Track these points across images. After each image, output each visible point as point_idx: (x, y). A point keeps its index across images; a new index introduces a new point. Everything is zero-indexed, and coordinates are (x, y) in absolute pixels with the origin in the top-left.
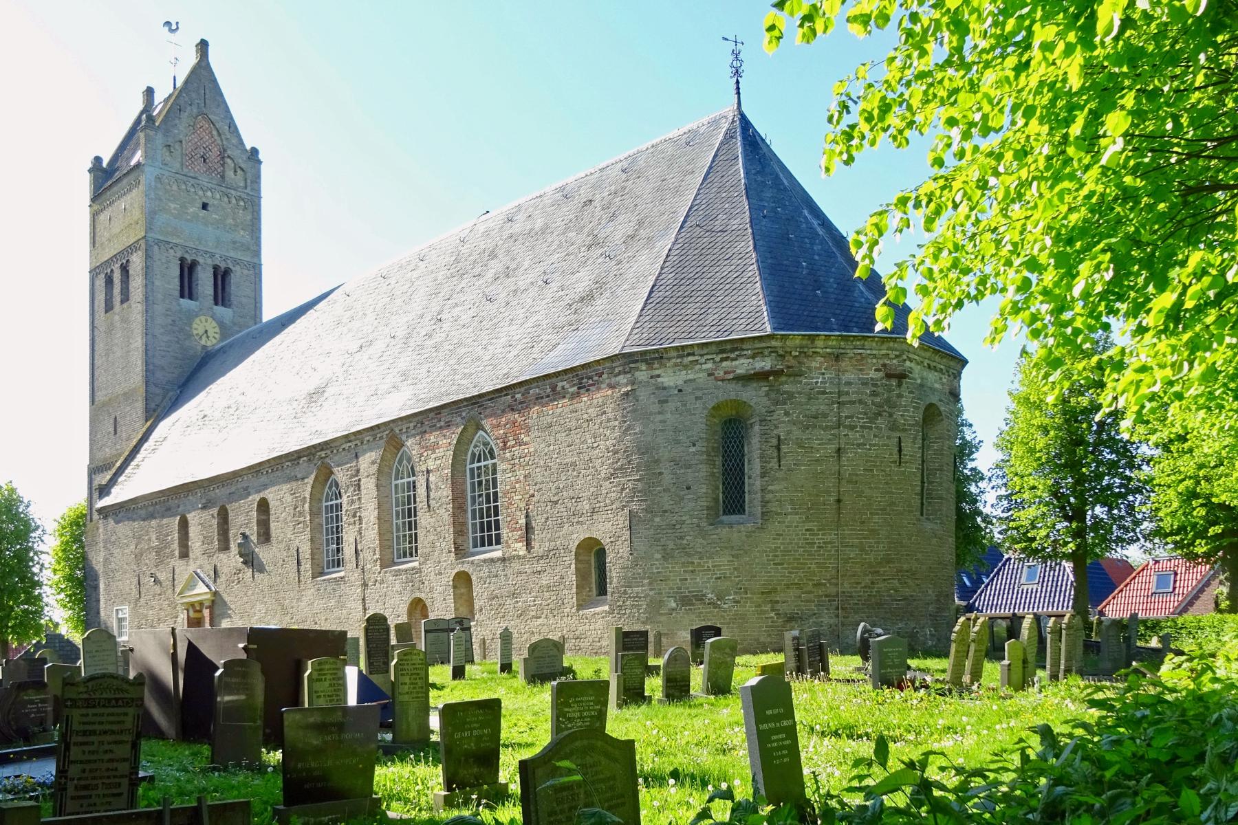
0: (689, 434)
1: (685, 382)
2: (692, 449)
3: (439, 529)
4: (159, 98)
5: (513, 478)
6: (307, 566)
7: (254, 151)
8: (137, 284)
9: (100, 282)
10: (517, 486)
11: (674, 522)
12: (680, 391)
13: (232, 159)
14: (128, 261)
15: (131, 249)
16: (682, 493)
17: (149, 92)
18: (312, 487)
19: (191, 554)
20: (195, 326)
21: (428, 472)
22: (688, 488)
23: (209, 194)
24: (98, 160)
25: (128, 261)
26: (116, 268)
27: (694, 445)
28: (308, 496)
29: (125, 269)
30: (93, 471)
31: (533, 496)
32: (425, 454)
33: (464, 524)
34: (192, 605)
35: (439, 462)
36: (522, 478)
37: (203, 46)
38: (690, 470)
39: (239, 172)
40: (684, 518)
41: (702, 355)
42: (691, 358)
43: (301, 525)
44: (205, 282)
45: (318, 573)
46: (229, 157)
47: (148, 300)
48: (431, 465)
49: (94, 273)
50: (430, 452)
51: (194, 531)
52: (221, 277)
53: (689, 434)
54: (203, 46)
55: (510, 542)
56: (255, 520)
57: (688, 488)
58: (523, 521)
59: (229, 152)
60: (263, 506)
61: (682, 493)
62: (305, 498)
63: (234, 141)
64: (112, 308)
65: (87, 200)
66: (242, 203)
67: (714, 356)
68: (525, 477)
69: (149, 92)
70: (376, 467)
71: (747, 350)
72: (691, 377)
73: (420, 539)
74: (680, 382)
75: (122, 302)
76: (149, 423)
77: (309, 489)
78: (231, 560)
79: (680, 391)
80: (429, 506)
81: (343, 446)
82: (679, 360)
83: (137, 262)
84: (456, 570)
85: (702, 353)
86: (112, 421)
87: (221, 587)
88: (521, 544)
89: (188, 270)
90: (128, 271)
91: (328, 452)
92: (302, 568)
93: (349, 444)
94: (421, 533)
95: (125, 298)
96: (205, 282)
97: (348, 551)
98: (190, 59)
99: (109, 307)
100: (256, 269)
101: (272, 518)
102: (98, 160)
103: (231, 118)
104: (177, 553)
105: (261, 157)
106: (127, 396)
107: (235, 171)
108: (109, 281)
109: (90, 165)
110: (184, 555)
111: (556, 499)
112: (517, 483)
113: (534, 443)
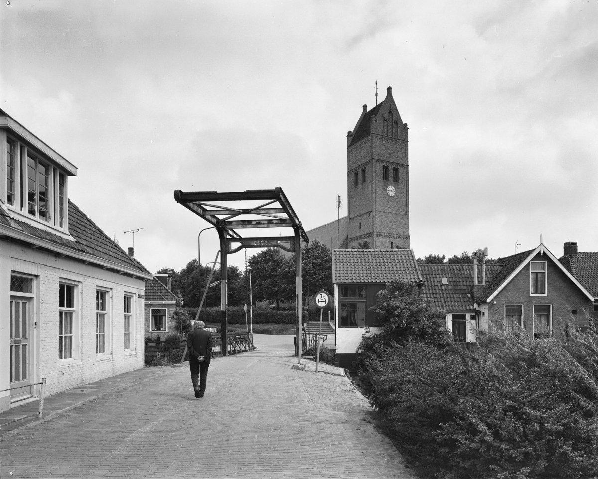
7: (406, 125)
9: (353, 176)
17: (365, 107)
20: (388, 187)
26: (360, 171)
29: (364, 171)
52: (396, 171)
65: (346, 147)
69: (365, 107)
89: (386, 169)
95: (364, 181)
96: (391, 171)
99: (356, 183)
100: (406, 166)
105: (408, 127)
108: (356, 174)
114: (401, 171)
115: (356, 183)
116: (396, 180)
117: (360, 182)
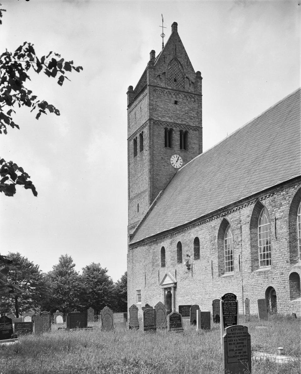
3: (282, 250)
4: (157, 55)
6: (216, 270)
8: (146, 143)
9: (132, 142)
14: (143, 132)
15: (143, 126)
17: (153, 52)
18: (219, 231)
19: (166, 265)
21: (276, 219)
24: (131, 87)
25: (143, 132)
26: (138, 135)
28: (217, 235)
29: (141, 135)
30: (130, 229)
32: (275, 210)
33: (296, 247)
34: (165, 289)
35: (282, 213)
37: (175, 25)
43: (214, 250)
44: (176, 137)
45: (221, 272)
47: (151, 147)
48: (278, 215)
49: (129, 140)
50: (278, 209)
51: (167, 254)
54: (175, 25)
56: (193, 249)
60: (197, 241)
62: (215, 236)
64: (136, 155)
69: (153, 52)
70: (249, 219)
73: (272, 256)
75: (141, 151)
76: (151, 205)
77: (218, 232)
78: (182, 268)
80: (276, 238)
81: (234, 209)
83: (146, 131)
84: (290, 273)
86: (137, 205)
87: (178, 281)
90: (142, 137)
92: (214, 271)
93: (236, 208)
94: (273, 252)
95: (142, 149)
96: (176, 137)
97: (236, 262)
98: (168, 33)
99: (135, 154)
101: (201, 247)
102: (131, 87)
104: (160, 264)
106: (144, 192)
109: (127, 91)
110: (163, 265)
114: (192, 134)
115: (135, 154)
116: (184, 146)
117: (138, 150)
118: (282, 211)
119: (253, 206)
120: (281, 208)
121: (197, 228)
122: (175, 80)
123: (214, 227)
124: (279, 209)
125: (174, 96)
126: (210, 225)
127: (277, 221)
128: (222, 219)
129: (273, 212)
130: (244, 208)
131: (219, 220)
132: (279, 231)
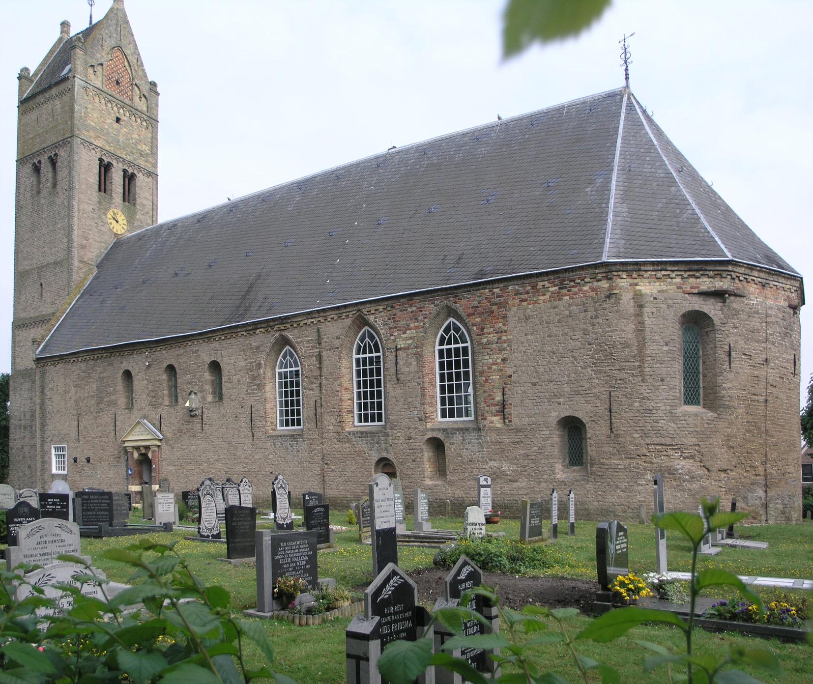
0: (663, 335)
1: (659, 292)
2: (666, 348)
5: (491, 361)
10: (494, 367)
11: (651, 408)
12: (655, 298)
13: (138, 87)
16: (658, 384)
22: (662, 380)
23: (121, 111)
27: (667, 345)
31: (510, 376)
35: (410, 342)
36: (499, 361)
38: (663, 365)
39: (143, 99)
40: (659, 405)
41: (673, 271)
42: (664, 273)
46: (136, 85)
48: (401, 344)
53: (663, 335)
55: (486, 415)
57: (662, 380)
58: (499, 398)
59: (136, 81)
61: (658, 384)
63: (141, 73)
66: (144, 124)
67: (682, 273)
68: (502, 360)
71: (710, 271)
72: (664, 288)
74: (655, 291)
79: (655, 298)
80: (398, 380)
82: (653, 273)
85: (673, 269)
88: (497, 418)
91: (289, 326)
103: (139, 55)
107: (140, 97)
111: (533, 380)
112: (494, 364)
113: (514, 329)
118: (411, 338)
119: (348, 322)
120: (408, 332)
121: (215, 345)
122: (118, 83)
123: (258, 348)
124: (404, 333)
125: (115, 108)
126: (248, 342)
127: (400, 353)
128: (277, 335)
129: (392, 338)
130: (328, 324)
131: (270, 336)
132: (404, 369)
